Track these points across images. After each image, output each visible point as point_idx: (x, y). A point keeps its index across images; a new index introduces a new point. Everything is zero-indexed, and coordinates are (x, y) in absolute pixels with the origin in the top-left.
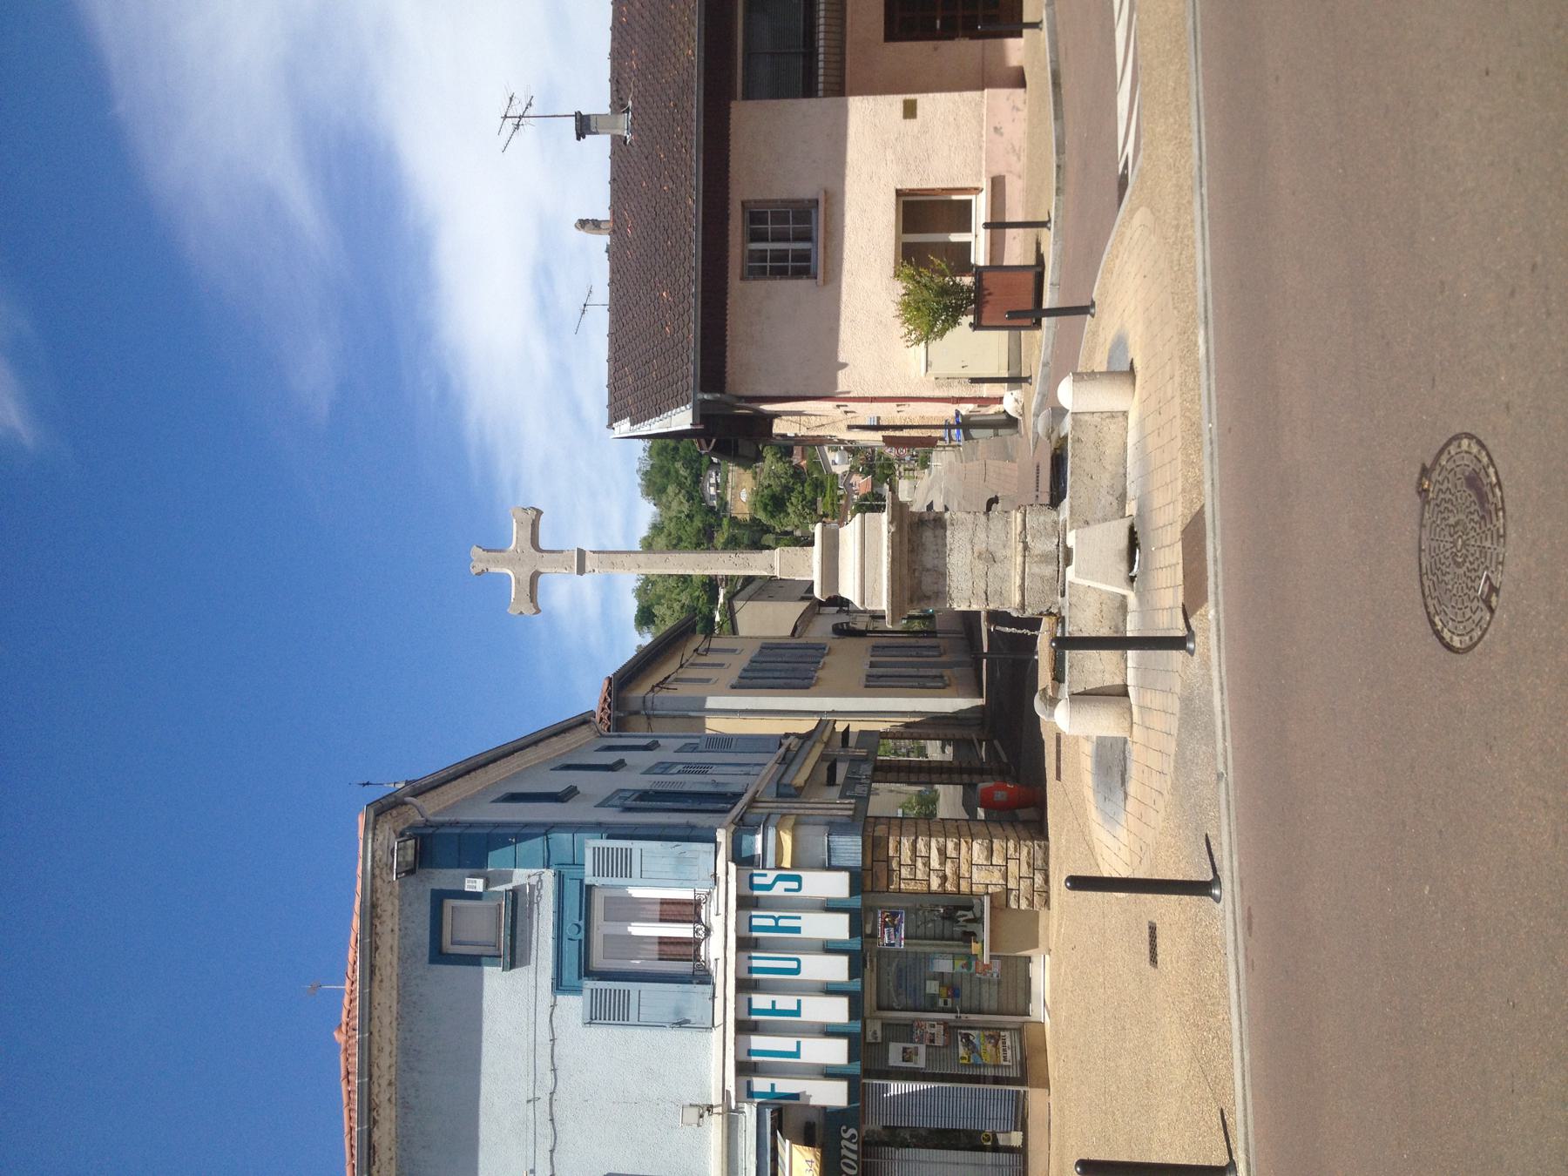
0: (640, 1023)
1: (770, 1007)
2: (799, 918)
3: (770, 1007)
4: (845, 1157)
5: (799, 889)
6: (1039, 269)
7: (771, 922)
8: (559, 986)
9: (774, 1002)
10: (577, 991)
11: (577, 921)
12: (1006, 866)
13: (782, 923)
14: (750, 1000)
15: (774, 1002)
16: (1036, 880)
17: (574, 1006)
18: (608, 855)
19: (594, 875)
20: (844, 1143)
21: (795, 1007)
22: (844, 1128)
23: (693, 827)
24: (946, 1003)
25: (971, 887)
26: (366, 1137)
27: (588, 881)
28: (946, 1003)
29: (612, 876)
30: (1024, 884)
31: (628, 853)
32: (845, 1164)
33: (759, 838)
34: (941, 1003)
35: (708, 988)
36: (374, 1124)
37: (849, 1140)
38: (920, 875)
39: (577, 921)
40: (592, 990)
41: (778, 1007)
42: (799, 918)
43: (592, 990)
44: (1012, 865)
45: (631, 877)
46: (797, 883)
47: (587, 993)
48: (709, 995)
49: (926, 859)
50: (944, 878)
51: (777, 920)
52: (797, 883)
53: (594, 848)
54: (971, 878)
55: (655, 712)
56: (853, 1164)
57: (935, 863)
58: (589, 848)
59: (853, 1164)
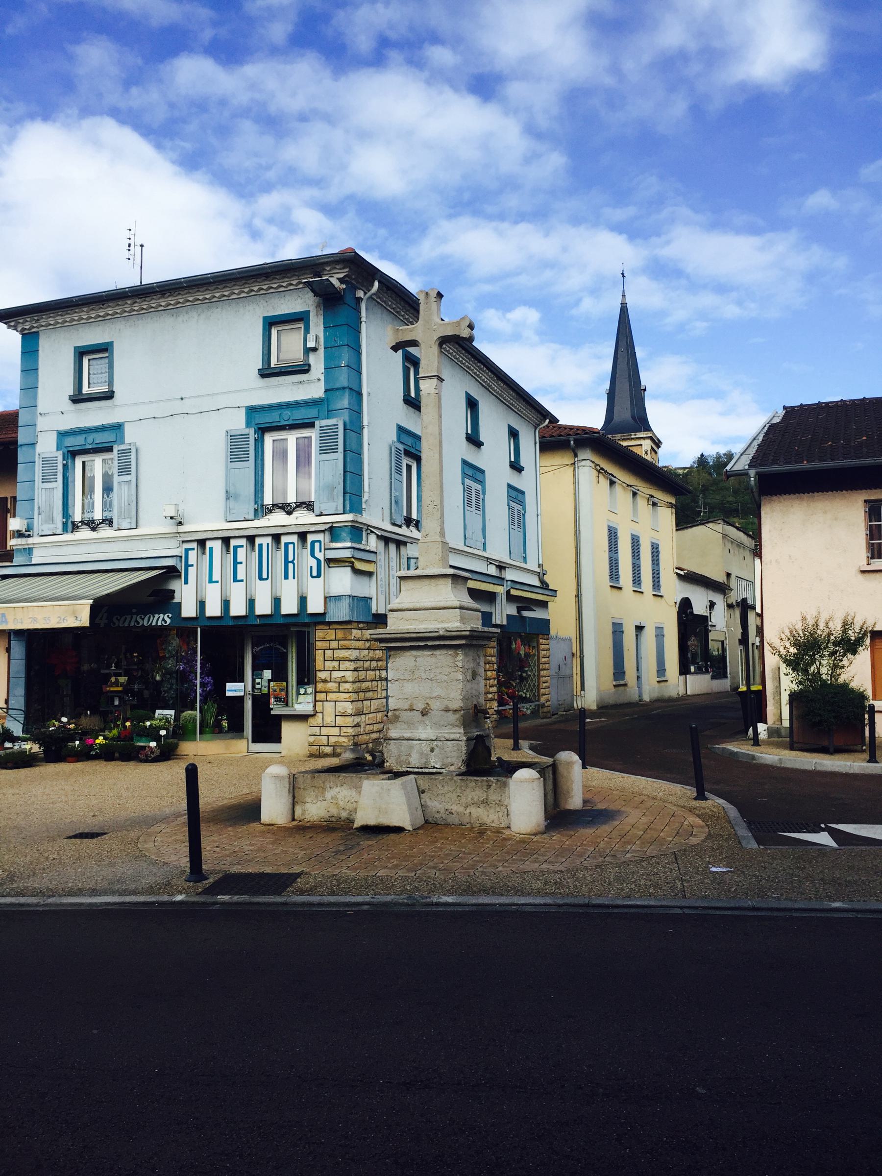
0: (229, 469)
1: (238, 561)
2: (294, 578)
3: (238, 561)
4: (154, 617)
5: (313, 577)
6: (831, 750)
7: (291, 559)
8: (252, 411)
9: (241, 563)
10: (248, 424)
11: (292, 418)
12: (335, 726)
13: (290, 565)
14: (242, 546)
15: (241, 563)
16: (327, 748)
17: (238, 422)
18: (327, 436)
19: (320, 427)
20: (162, 615)
21: (238, 578)
22: (170, 616)
23: (92, 491)
24: (258, 684)
25: (321, 701)
26: (152, 291)
27: (317, 423)
28: (258, 684)
29: (320, 440)
30: (324, 740)
31: (334, 450)
32: (150, 617)
33: (349, 544)
34: (258, 680)
35: (251, 516)
36: (162, 294)
37: (163, 620)
38: (328, 664)
39: (292, 418)
40: (249, 434)
41: (189, 568)
42: (294, 578)
43: (249, 434)
44: (336, 731)
45: (320, 454)
46: (316, 575)
47: (246, 431)
48: (247, 517)
49: (338, 668)
50: (325, 681)
51: (292, 562)
52: (316, 575)
53: (337, 425)
54: (327, 701)
55: (576, 468)
56: (150, 623)
57: (336, 674)
58: (337, 422)
59: (150, 623)
